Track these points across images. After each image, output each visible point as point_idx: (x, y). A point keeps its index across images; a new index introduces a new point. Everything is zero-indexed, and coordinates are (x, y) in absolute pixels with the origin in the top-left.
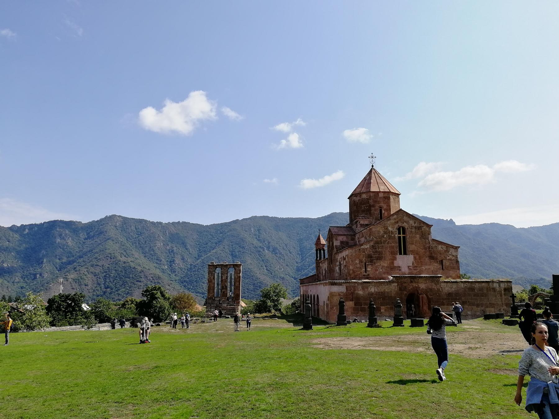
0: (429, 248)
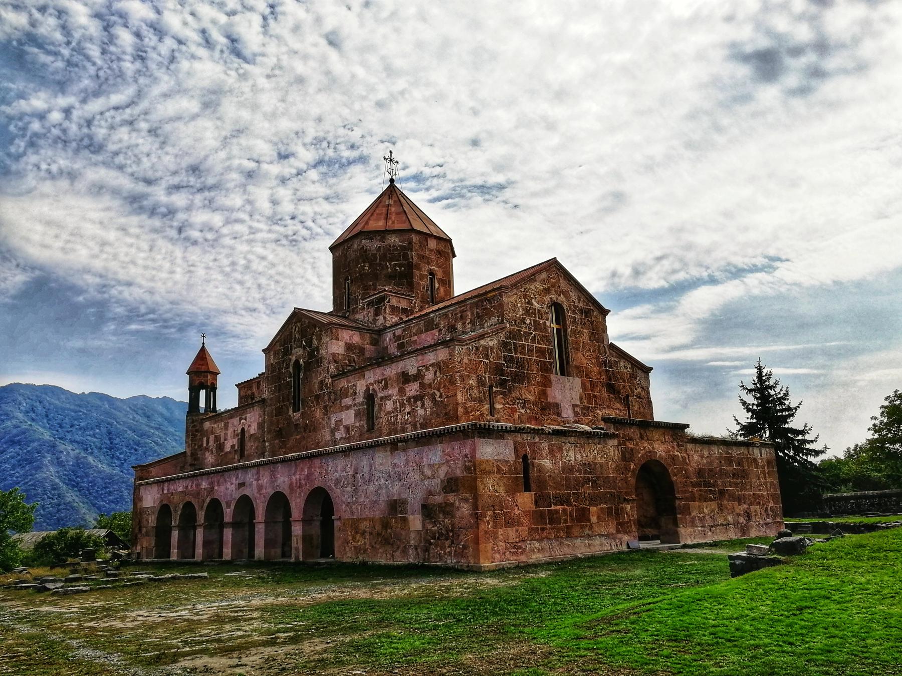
0: (605, 362)
